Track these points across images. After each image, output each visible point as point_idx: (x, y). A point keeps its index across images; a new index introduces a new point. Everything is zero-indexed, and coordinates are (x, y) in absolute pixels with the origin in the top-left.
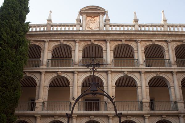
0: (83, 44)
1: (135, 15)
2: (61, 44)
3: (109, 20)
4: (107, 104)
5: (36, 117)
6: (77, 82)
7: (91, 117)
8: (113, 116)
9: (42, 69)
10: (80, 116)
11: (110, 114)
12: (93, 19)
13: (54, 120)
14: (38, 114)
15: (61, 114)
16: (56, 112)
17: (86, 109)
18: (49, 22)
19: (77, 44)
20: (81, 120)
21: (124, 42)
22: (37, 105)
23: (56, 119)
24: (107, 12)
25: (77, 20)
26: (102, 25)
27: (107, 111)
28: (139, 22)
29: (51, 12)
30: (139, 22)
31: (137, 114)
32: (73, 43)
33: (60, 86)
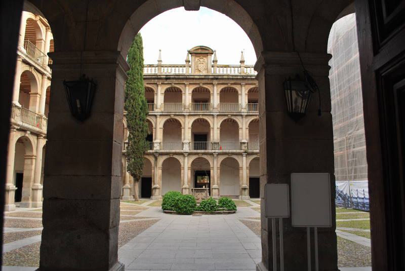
0: (193, 87)
1: (242, 55)
2: (172, 87)
3: (216, 61)
6: (187, 124)
9: (158, 112)
10: (190, 154)
11: (215, 153)
12: (201, 60)
15: (176, 152)
16: (171, 151)
17: (195, 149)
18: (160, 63)
19: (187, 87)
21: (229, 85)
22: (155, 145)
24: (215, 51)
25: (186, 61)
26: (210, 66)
28: (246, 63)
29: (160, 51)
30: (246, 63)
32: (183, 86)
33: (173, 128)
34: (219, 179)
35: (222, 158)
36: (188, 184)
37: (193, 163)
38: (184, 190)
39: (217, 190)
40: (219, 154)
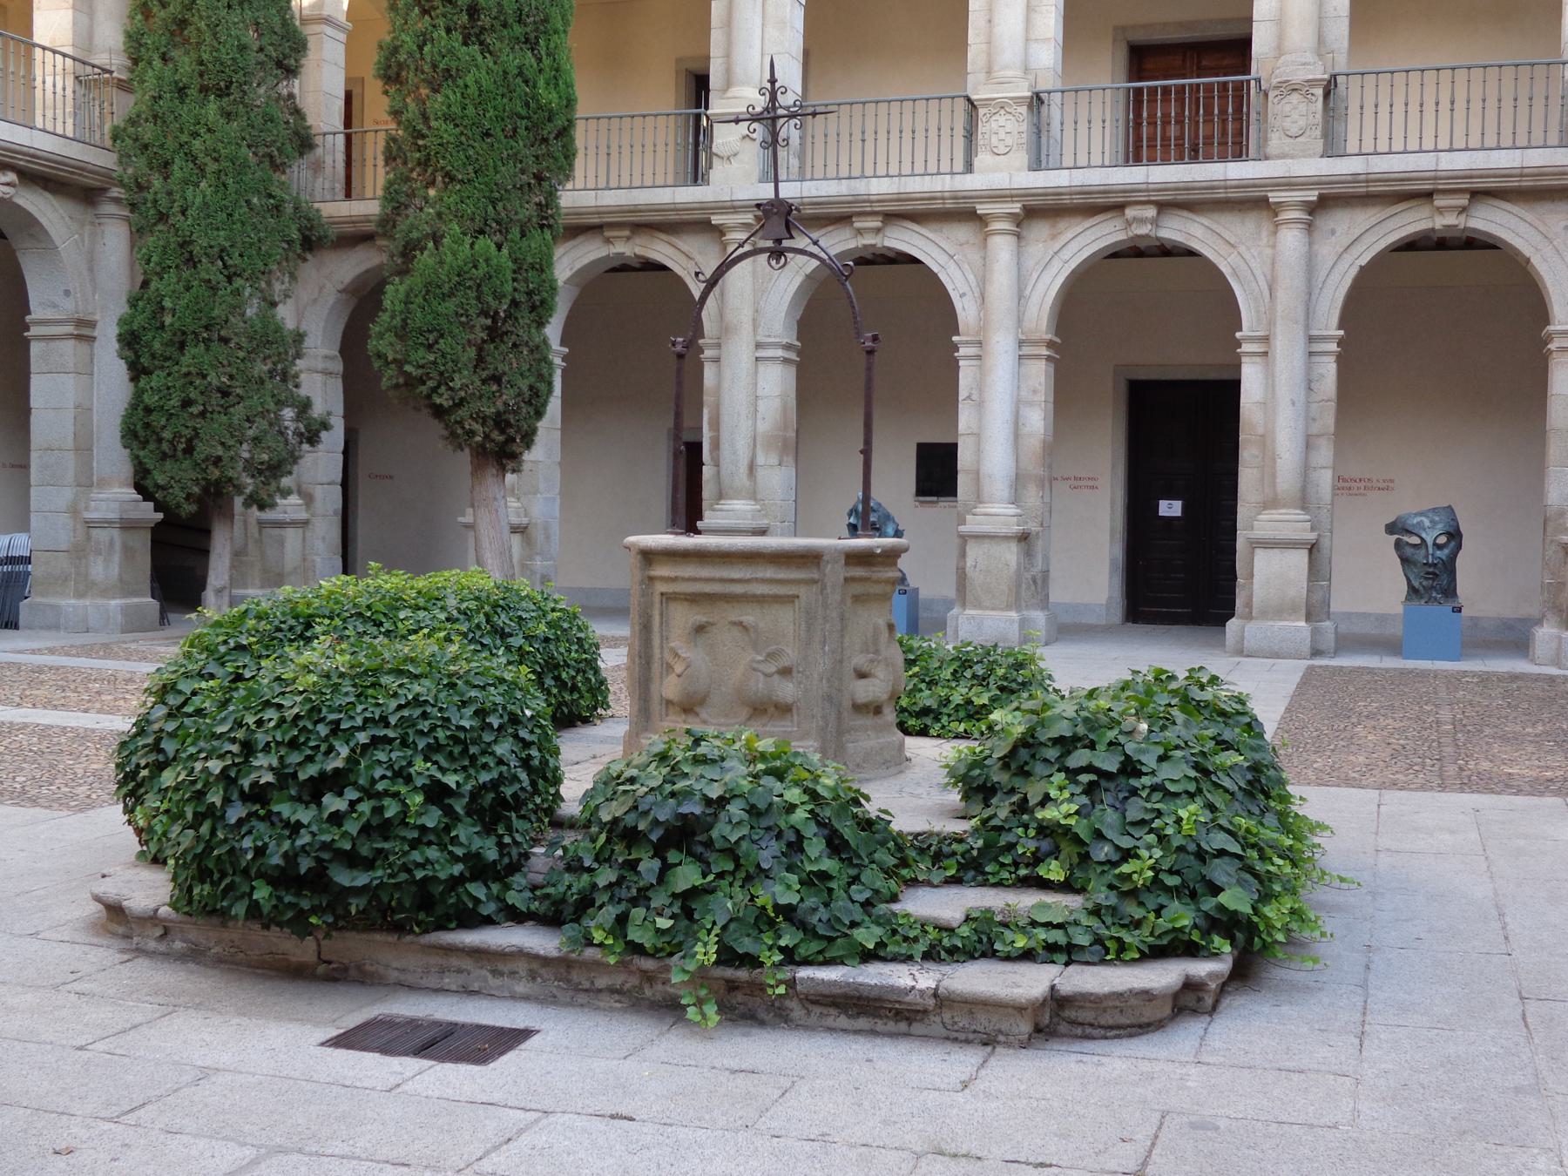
4: (1266, 95)
5: (719, 231)
7: (1130, 212)
8: (1312, 196)
10: (1040, 211)
11: (1289, 184)
13: (852, 245)
14: (733, 208)
15: (901, 198)
20: (1054, 237)
22: (725, 138)
23: (869, 240)
27: (1267, 158)
31: (1522, 173)
34: (1324, 454)
35: (1361, 239)
36: (1015, 500)
37: (1080, 301)
38: (974, 552)
39: (1300, 558)
40: (1328, 201)
